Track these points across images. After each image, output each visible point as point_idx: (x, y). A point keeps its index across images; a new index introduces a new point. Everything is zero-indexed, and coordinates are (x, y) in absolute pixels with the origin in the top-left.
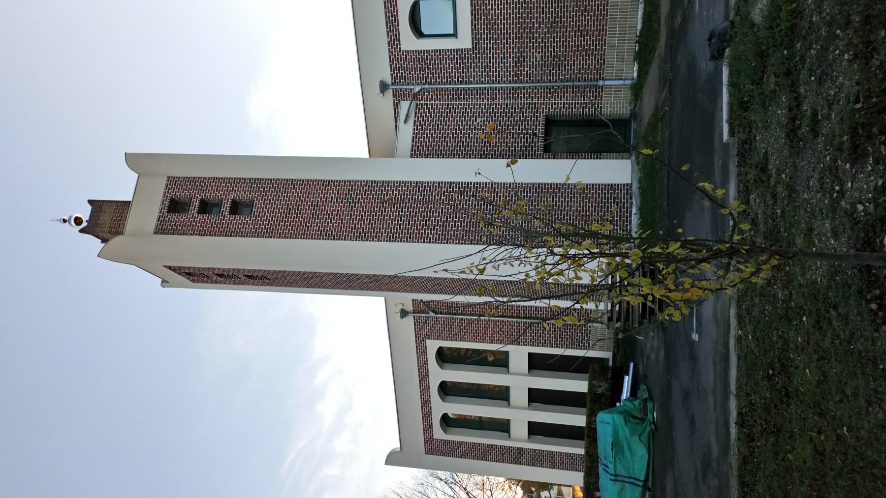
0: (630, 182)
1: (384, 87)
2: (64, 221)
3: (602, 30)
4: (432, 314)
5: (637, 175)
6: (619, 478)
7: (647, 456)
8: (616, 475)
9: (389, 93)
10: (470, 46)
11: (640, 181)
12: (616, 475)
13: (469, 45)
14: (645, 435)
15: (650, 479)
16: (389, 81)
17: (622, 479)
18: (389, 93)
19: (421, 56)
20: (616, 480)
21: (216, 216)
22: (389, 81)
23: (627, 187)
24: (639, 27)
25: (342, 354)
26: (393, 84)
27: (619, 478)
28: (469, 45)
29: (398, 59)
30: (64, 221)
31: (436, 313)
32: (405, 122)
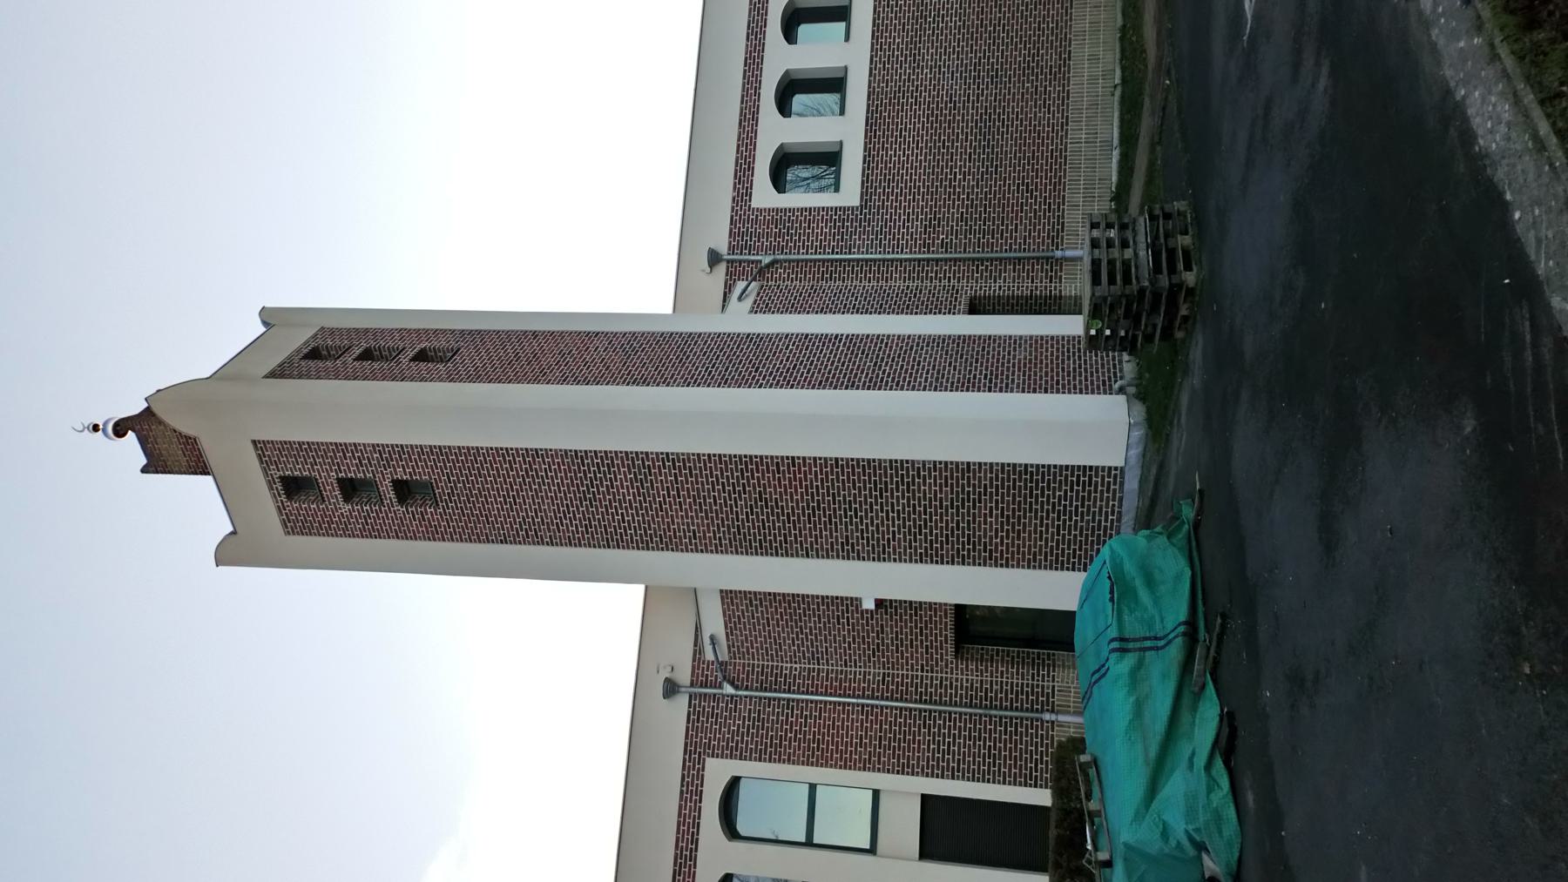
0: (1121, 463)
1: (714, 258)
2: (96, 428)
3: (1058, 185)
4: (729, 689)
5: (1135, 452)
6: (1131, 645)
7: (1188, 573)
8: (1122, 639)
9: (722, 269)
10: (857, 203)
11: (1145, 467)
12: (1122, 639)
13: (856, 202)
14: (1182, 535)
15: (1200, 596)
16: (723, 248)
17: (1138, 645)
18: (722, 269)
19: (781, 217)
20: (1123, 650)
21: (367, 446)
22: (723, 248)
23: (1116, 474)
24: (1114, 179)
25: (529, 685)
26: (692, 685)
27: (1131, 645)
28: (856, 202)
29: (746, 222)
30: (96, 428)
31: (737, 688)
32: (740, 299)
